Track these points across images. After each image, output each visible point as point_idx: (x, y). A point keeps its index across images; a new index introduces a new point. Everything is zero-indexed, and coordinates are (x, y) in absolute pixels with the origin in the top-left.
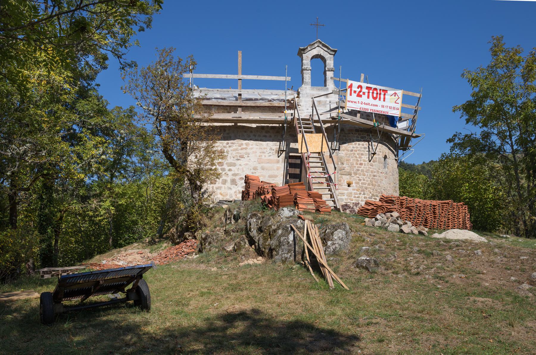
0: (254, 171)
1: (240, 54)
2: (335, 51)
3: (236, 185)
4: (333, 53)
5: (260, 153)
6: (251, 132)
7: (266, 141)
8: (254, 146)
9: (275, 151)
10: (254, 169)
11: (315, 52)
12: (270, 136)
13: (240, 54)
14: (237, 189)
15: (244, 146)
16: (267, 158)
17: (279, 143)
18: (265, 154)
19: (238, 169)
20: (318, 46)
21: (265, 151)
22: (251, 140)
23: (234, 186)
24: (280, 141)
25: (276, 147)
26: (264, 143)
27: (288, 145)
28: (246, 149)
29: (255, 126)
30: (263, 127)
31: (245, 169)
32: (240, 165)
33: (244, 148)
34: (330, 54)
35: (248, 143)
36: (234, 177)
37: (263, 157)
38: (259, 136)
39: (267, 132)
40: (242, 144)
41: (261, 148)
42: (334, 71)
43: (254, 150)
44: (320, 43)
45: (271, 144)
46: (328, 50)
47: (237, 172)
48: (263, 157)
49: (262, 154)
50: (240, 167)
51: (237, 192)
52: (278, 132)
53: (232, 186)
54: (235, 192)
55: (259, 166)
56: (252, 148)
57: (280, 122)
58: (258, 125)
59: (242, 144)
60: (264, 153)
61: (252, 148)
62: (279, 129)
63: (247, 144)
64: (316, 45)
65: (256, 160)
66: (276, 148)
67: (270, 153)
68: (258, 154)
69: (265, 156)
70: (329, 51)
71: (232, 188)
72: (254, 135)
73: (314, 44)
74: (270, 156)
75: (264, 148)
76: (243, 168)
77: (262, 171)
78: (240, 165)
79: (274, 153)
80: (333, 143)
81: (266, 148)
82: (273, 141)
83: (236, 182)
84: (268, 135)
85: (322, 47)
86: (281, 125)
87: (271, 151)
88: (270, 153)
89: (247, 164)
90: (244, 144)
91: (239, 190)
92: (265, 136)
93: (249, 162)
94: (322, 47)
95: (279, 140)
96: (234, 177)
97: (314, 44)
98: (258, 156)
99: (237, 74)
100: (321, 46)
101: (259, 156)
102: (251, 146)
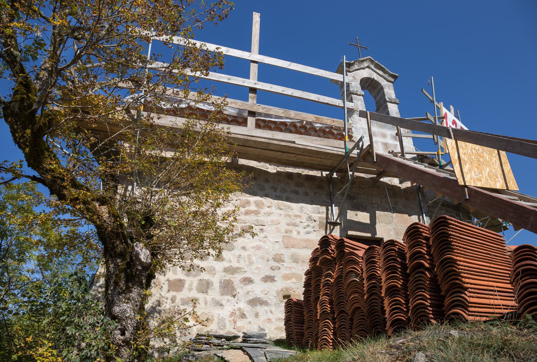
0: (275, 264)
1: (256, 17)
2: (395, 77)
3: (234, 296)
4: (393, 80)
5: (288, 225)
6: (267, 181)
7: (297, 202)
8: (273, 209)
9: (318, 223)
10: (275, 260)
11: (366, 73)
12: (306, 194)
13: (256, 17)
14: (237, 306)
15: (253, 207)
16: (303, 236)
17: (324, 209)
18: (297, 228)
19: (240, 256)
20: (368, 67)
21: (298, 221)
22: (267, 196)
23: (229, 297)
24: (327, 203)
25: (319, 215)
26: (296, 207)
27: (342, 214)
28: (257, 213)
29: (275, 171)
30: (290, 175)
31: (254, 258)
32: (244, 248)
33: (252, 212)
34: (388, 81)
35: (261, 201)
36: (228, 277)
37: (294, 234)
38: (284, 190)
39: (298, 185)
40: (248, 203)
41: (290, 216)
42: (397, 104)
43: (274, 218)
44: (372, 61)
45: (309, 208)
46: (384, 75)
47: (235, 264)
48: (294, 234)
49: (291, 228)
50: (244, 254)
51: (238, 313)
52: (320, 187)
53: (224, 299)
54: (233, 314)
55: (287, 253)
56: (269, 214)
57: (328, 163)
58: (281, 169)
59: (248, 203)
60: (295, 225)
61: (269, 214)
62: (322, 181)
63: (257, 204)
64: (366, 64)
65: (280, 239)
66: (320, 218)
67: (308, 226)
68: (283, 227)
69: (299, 233)
70: (386, 76)
71: (224, 303)
72: (272, 188)
73: (363, 61)
74: (308, 233)
75: (296, 216)
76: (249, 256)
77: (294, 265)
78: (244, 248)
79: (317, 228)
80: (421, 217)
81: (299, 216)
82: (312, 203)
83: (233, 289)
84: (301, 190)
85: (375, 69)
86: (325, 173)
87: (309, 223)
88: (308, 226)
89: (258, 248)
90: (252, 202)
91: (240, 309)
92: (296, 193)
93: (264, 242)
94: (375, 69)
95: (324, 202)
96: (228, 277)
97: (363, 61)
98: (283, 230)
99: (248, 49)
100: (372, 66)
101: (286, 232)
102: (267, 210)
